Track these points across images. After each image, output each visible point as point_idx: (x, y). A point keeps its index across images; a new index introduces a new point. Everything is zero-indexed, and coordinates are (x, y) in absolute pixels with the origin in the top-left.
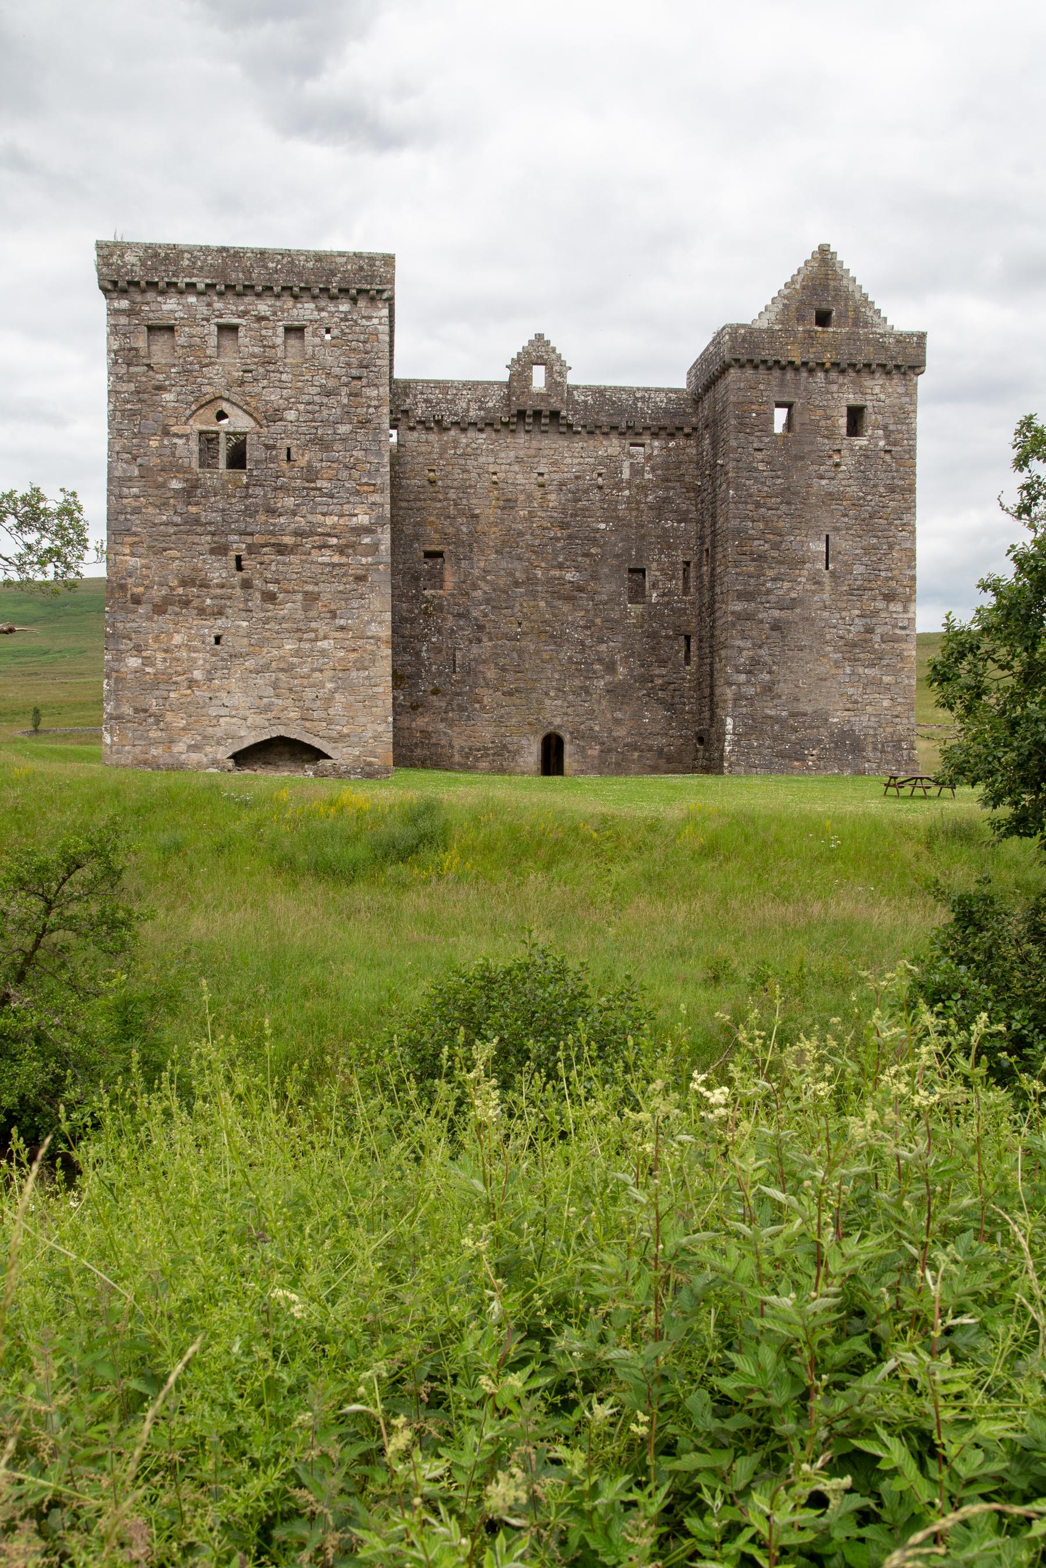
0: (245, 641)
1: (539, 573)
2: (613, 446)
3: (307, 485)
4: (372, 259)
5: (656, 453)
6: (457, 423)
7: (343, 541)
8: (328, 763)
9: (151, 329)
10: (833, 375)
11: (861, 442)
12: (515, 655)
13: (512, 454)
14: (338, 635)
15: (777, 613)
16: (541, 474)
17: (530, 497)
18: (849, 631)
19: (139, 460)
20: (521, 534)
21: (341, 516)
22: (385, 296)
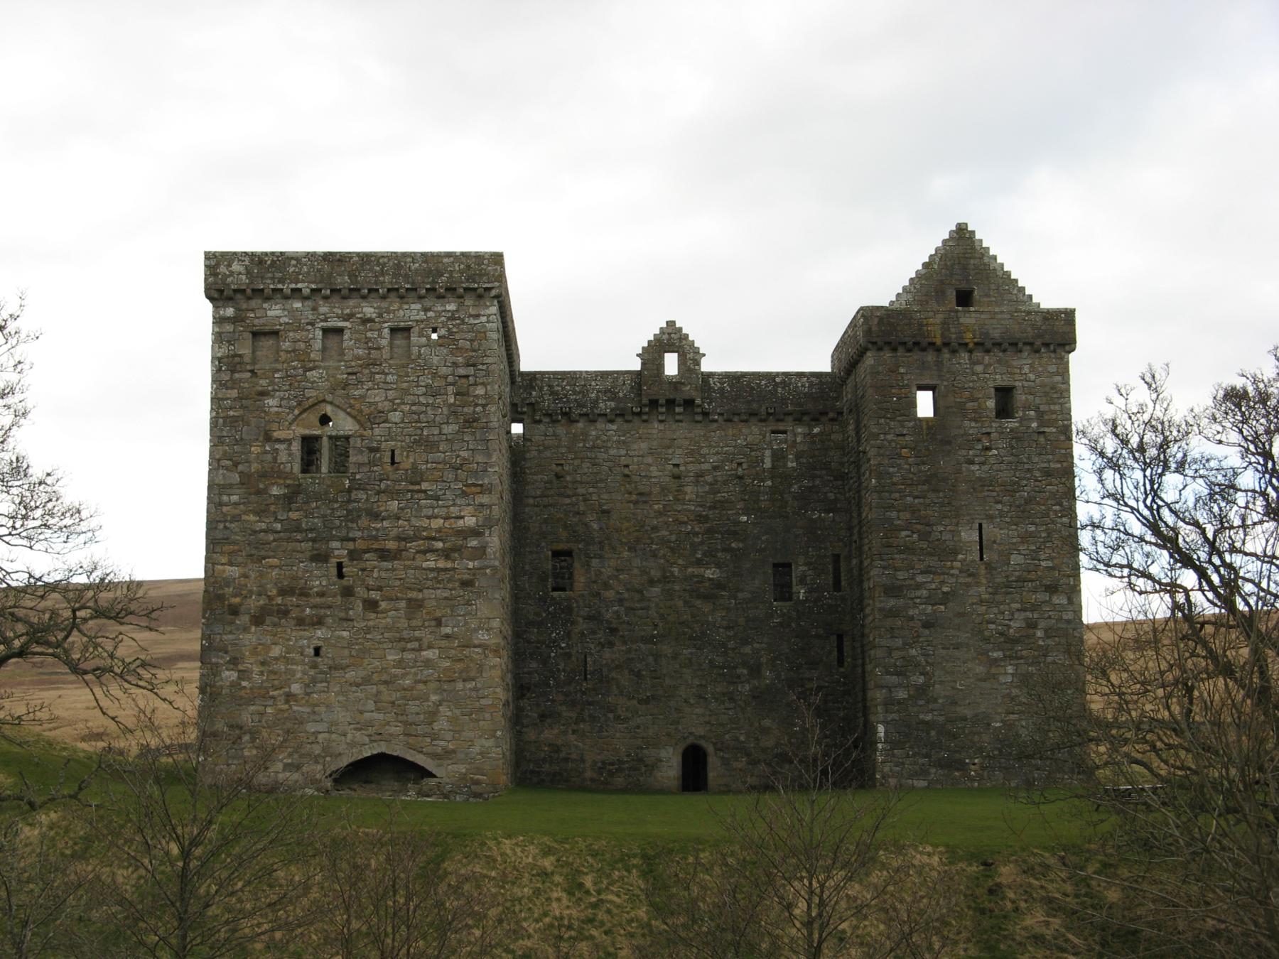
0: (346, 652)
1: (676, 571)
2: (752, 433)
3: (411, 487)
4: (479, 257)
5: (799, 440)
6: (586, 415)
7: (447, 545)
8: (432, 782)
9: (255, 335)
10: (978, 355)
11: (1012, 424)
12: (651, 659)
14: (444, 643)
15: (929, 609)
16: (677, 466)
17: (665, 490)
18: (1009, 627)
19: (240, 468)
20: (655, 529)
21: (446, 518)
22: (493, 293)
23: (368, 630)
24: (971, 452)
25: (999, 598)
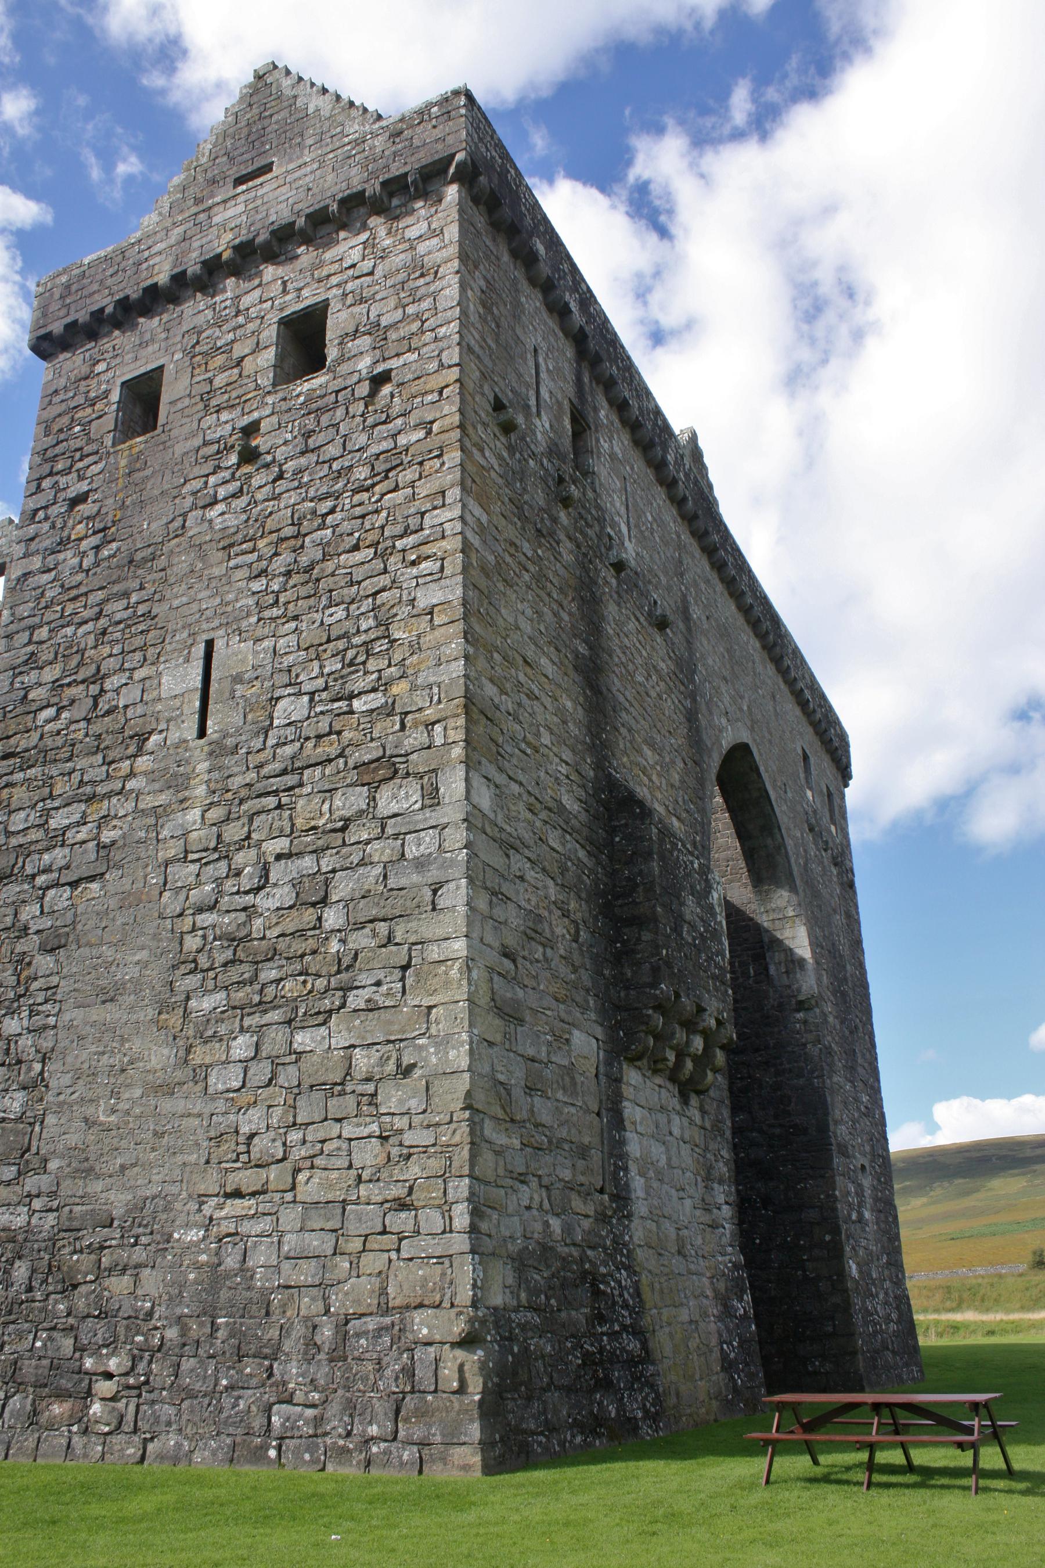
24: (212, 480)
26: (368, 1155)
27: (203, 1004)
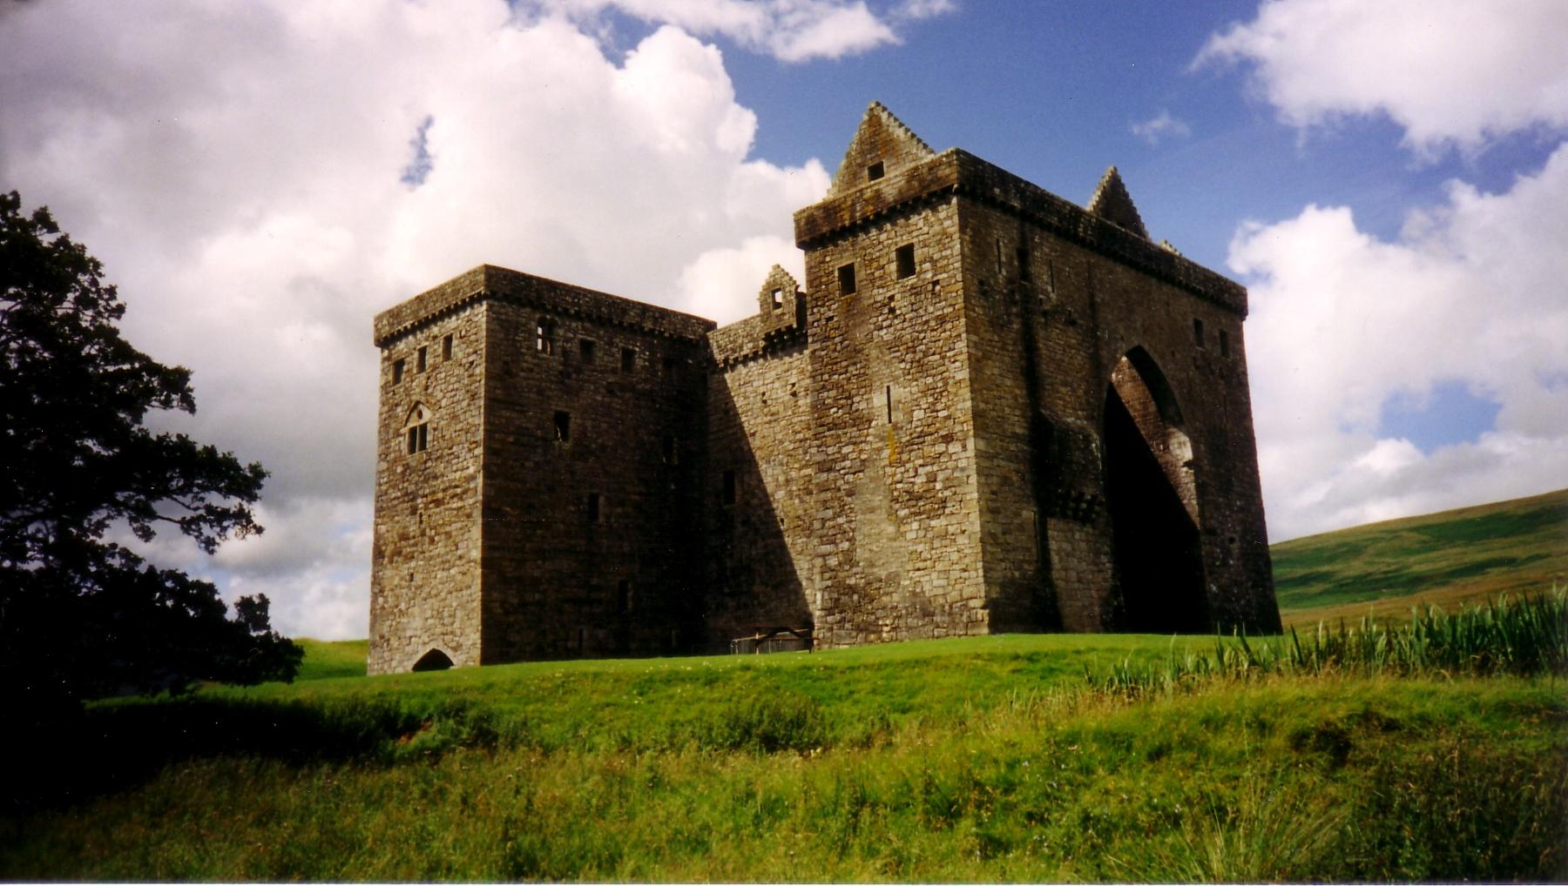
11: (912, 280)
13: (773, 373)
14: (458, 562)
16: (794, 385)
20: (781, 442)
21: (462, 470)
23: (431, 558)
24: (880, 319)
25: (905, 457)
26: (955, 557)
27: (902, 513)
